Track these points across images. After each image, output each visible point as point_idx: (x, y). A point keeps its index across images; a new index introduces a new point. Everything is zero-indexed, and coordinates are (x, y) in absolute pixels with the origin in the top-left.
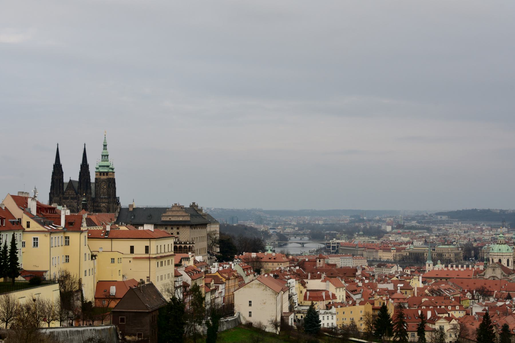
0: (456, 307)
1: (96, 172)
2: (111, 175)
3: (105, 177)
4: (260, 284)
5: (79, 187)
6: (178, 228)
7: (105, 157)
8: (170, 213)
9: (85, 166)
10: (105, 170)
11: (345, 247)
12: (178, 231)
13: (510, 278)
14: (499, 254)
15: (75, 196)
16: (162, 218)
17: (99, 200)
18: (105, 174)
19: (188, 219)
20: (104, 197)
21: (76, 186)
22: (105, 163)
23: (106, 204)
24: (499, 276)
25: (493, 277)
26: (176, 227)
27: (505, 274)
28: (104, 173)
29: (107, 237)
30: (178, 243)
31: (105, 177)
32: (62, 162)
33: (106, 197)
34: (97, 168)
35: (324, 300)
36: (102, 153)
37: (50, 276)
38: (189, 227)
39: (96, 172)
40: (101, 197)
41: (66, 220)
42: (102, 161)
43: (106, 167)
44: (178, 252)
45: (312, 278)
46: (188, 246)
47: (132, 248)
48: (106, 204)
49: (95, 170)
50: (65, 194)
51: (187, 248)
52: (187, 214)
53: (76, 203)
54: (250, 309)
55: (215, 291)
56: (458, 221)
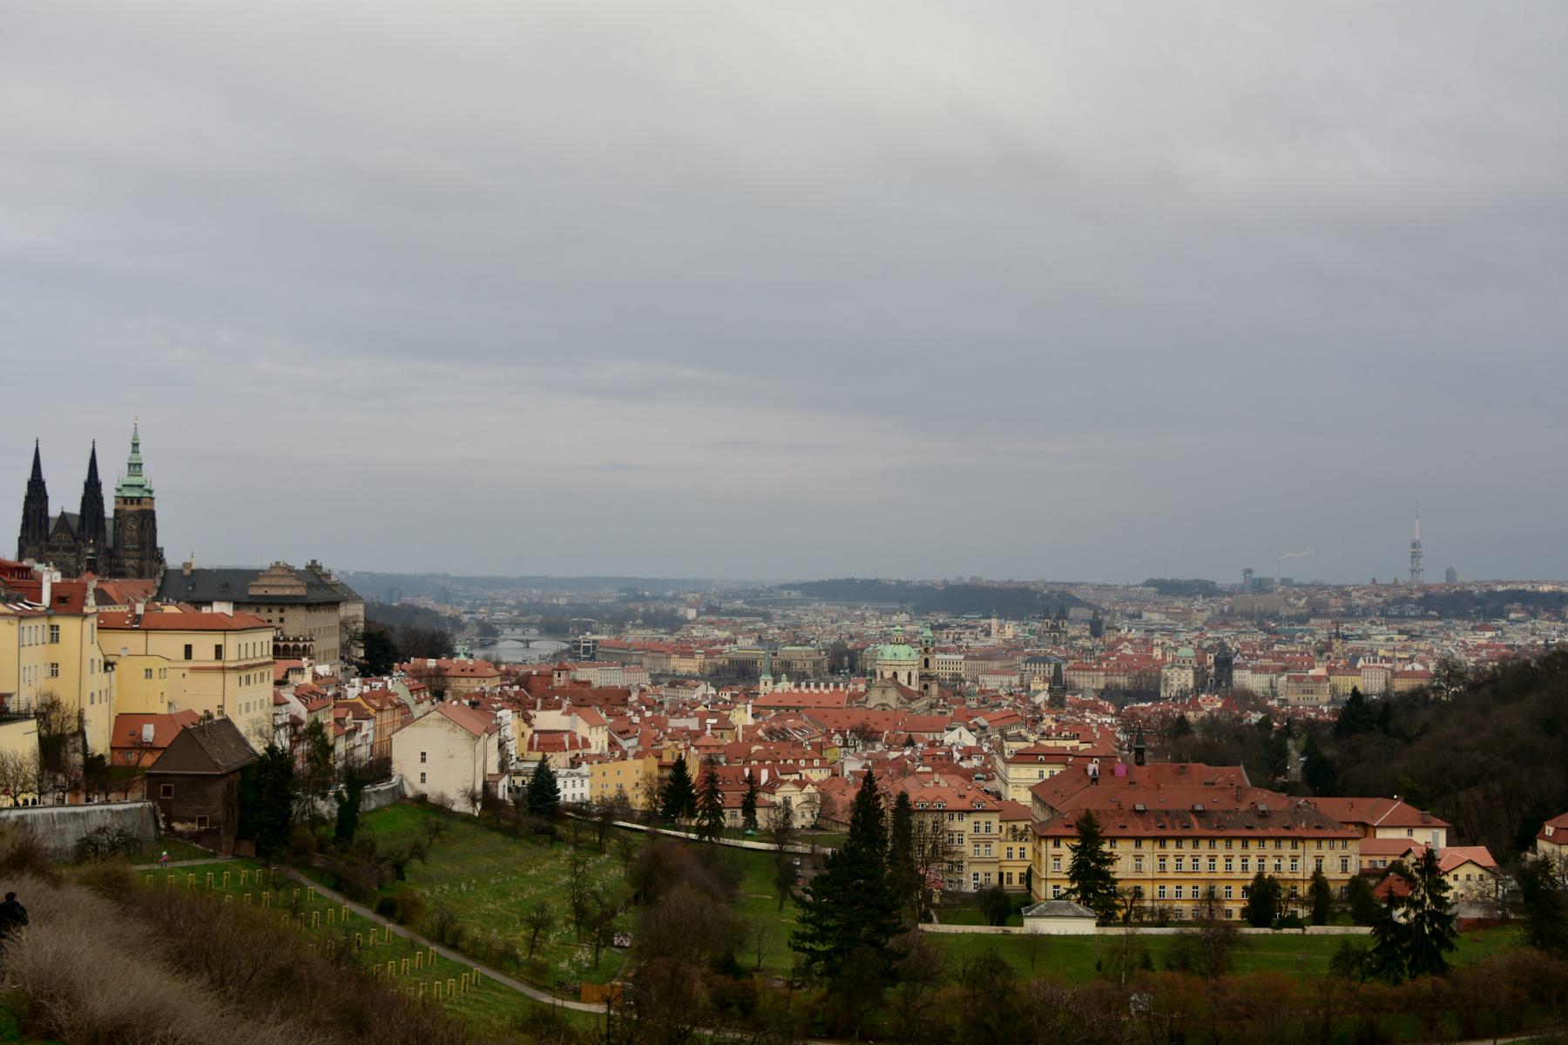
0: (815, 761)
1: (116, 497)
3: (135, 508)
4: (443, 719)
5: (82, 527)
7: (135, 467)
8: (266, 581)
9: (93, 486)
10: (136, 493)
11: (607, 648)
12: (282, 615)
13: (913, 707)
14: (893, 663)
15: (73, 544)
17: (122, 553)
19: (302, 592)
20: (131, 546)
21: (75, 524)
22: (136, 480)
23: (137, 561)
24: (893, 705)
25: (883, 705)
26: (278, 608)
27: (904, 700)
28: (132, 500)
30: (281, 639)
31: (135, 508)
32: (45, 475)
33: (136, 546)
34: (118, 490)
35: (566, 751)
36: (130, 459)
37: (19, 704)
38: (304, 608)
39: (116, 497)
40: (127, 546)
41: (52, 593)
42: (129, 475)
43: (136, 488)
44: (281, 657)
45: (544, 708)
46: (301, 645)
47: (188, 649)
49: (115, 493)
50: (52, 540)
51: (299, 650)
52: (300, 583)
54: (423, 768)
55: (355, 734)
56: (821, 600)
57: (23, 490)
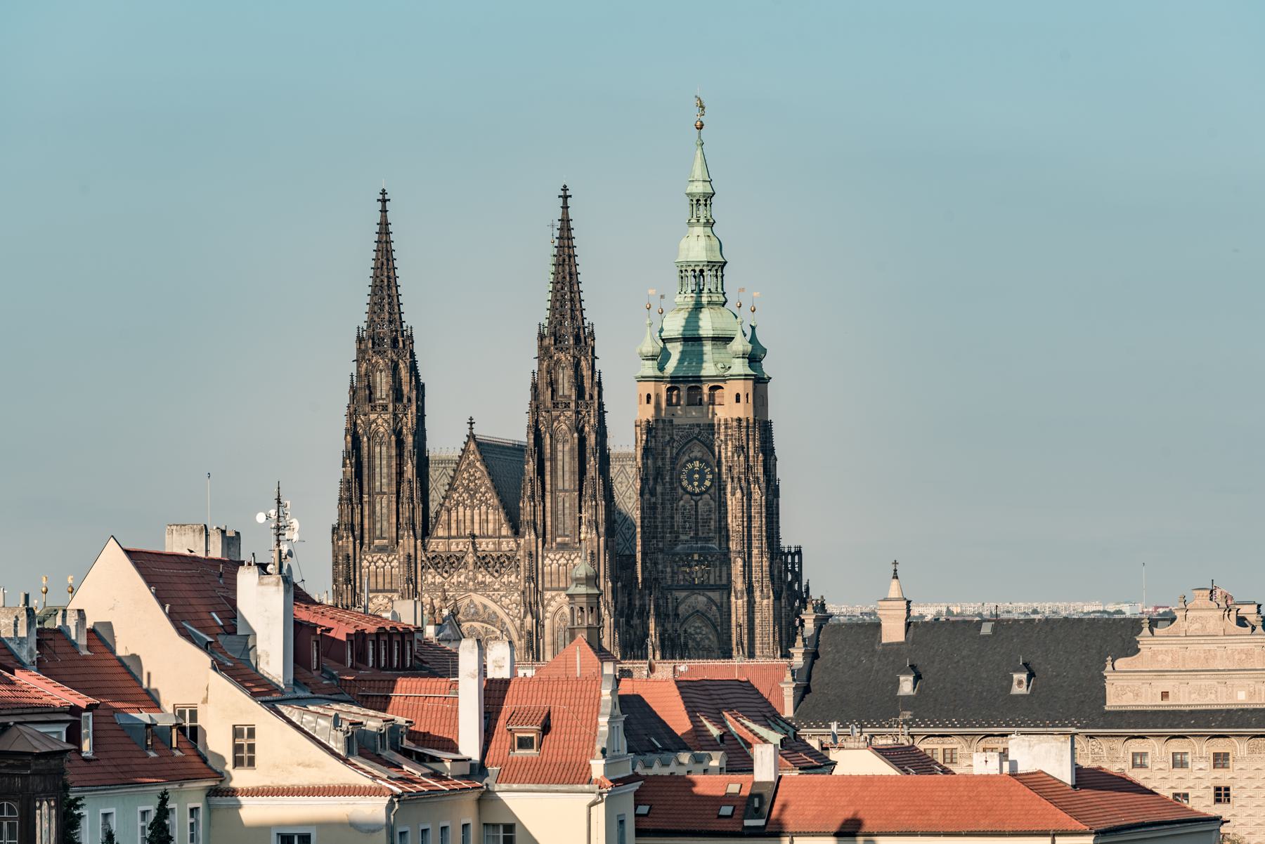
2: (742, 399)
15: (508, 545)
29: (761, 822)
48: (709, 598)
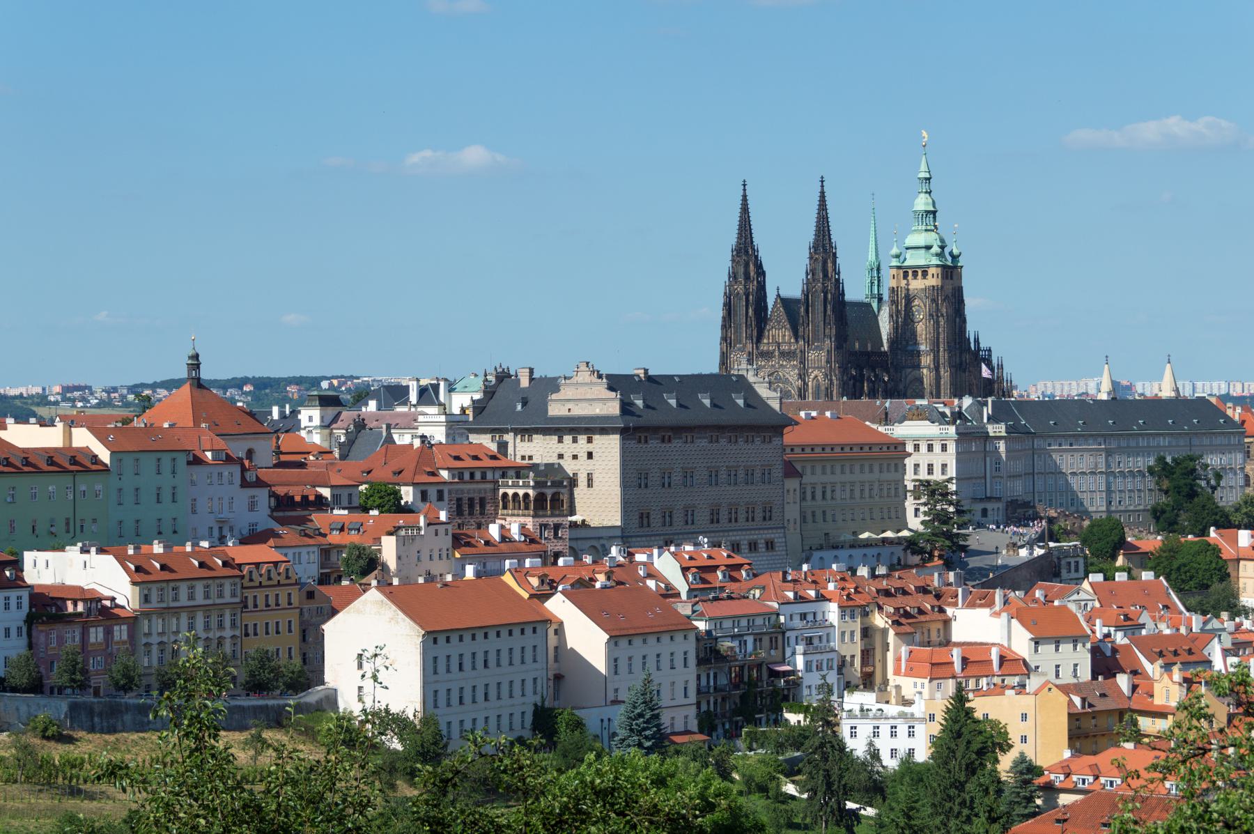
2: (935, 276)
6: (590, 441)
12: (590, 447)
16: (549, 408)
18: (920, 273)
26: (585, 437)
32: (757, 240)
43: (923, 251)
50: (765, 341)
53: (796, 371)
57: (724, 263)
